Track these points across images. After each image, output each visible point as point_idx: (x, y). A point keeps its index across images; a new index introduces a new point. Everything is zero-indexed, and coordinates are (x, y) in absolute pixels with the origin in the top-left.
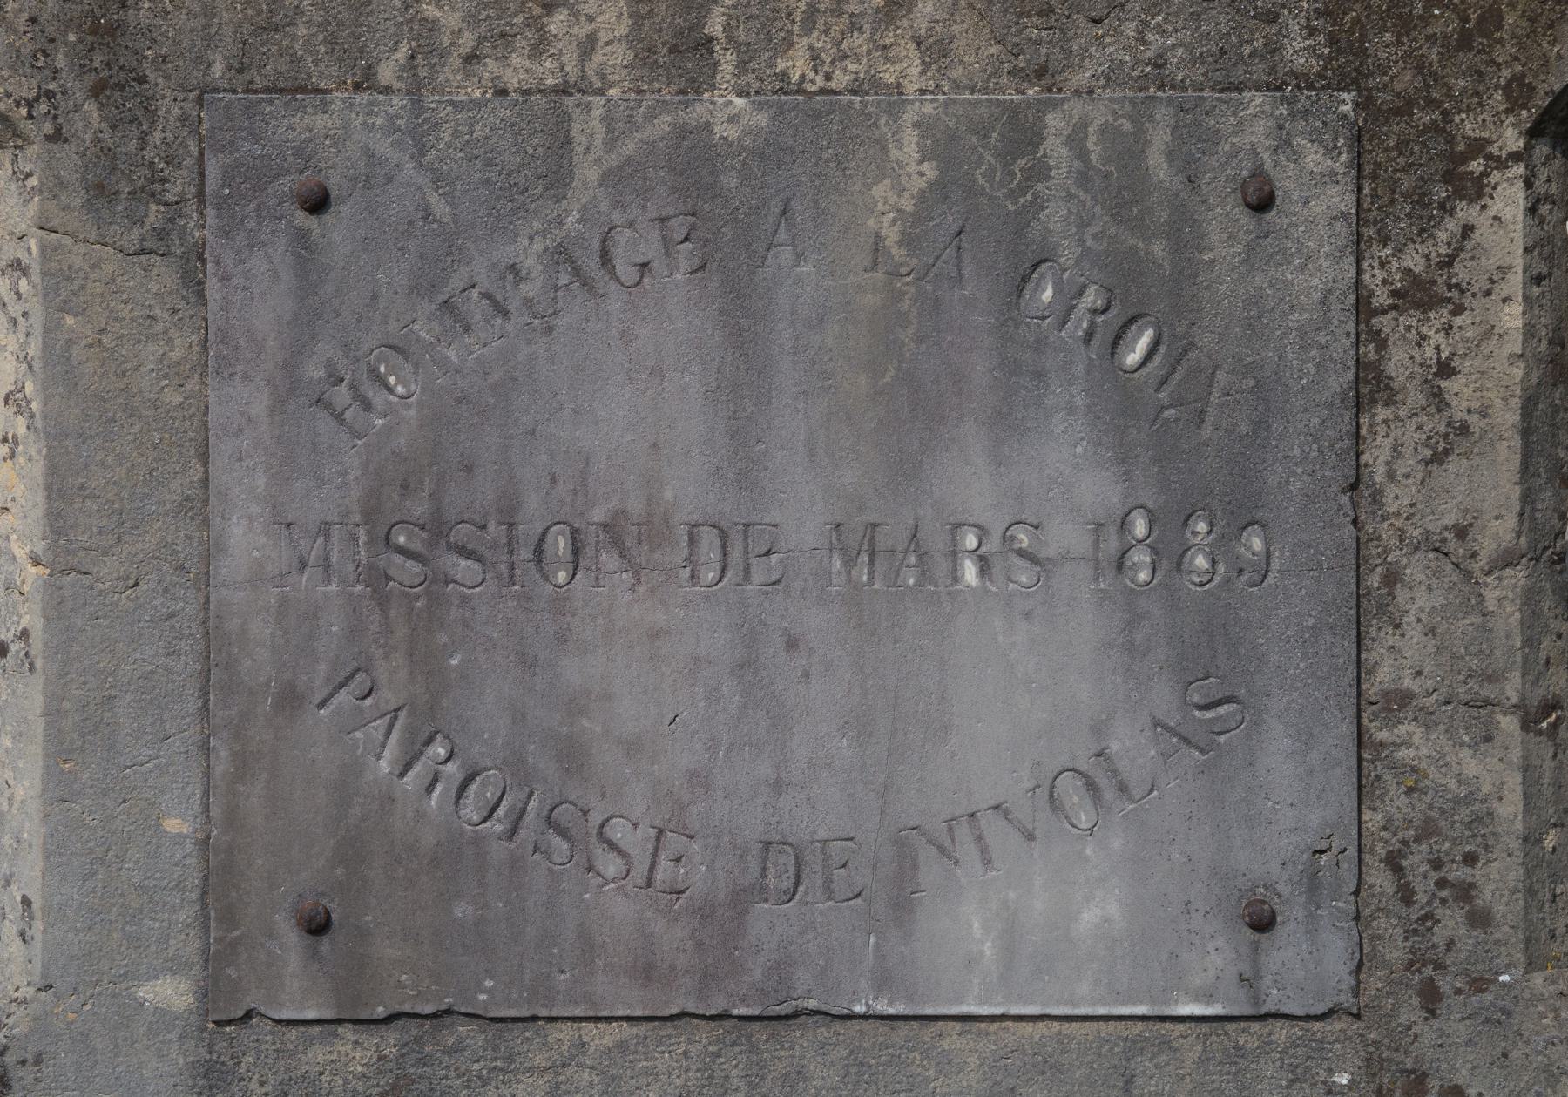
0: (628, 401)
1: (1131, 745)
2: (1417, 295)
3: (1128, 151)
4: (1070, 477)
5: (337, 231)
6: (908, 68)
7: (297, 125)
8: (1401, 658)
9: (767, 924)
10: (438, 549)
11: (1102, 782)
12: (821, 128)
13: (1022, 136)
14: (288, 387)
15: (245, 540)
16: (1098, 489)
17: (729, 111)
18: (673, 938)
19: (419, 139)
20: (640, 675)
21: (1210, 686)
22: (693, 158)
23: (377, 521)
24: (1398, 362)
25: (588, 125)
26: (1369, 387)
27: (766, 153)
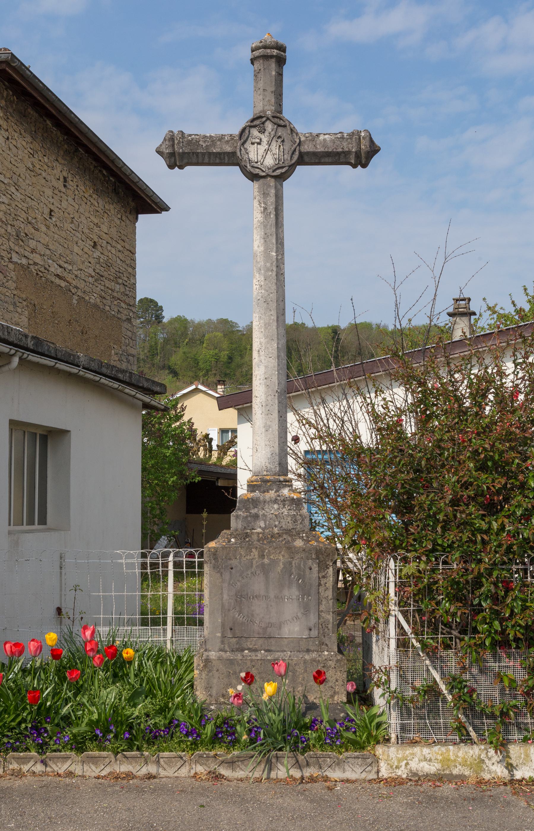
0: (258, 585)
1: (300, 615)
2: (324, 577)
3: (300, 565)
4: (295, 592)
5: (233, 571)
6: (281, 557)
8: (322, 608)
9: (269, 630)
10: (241, 597)
11: (297, 618)
12: (274, 562)
13: (291, 563)
14: (229, 584)
15: (225, 597)
16: (297, 593)
17: (266, 561)
18: (261, 631)
19: (240, 563)
20: (258, 608)
21: (306, 609)
22: (263, 565)
23: (236, 595)
24: (322, 583)
25: (254, 562)
27: (269, 565)
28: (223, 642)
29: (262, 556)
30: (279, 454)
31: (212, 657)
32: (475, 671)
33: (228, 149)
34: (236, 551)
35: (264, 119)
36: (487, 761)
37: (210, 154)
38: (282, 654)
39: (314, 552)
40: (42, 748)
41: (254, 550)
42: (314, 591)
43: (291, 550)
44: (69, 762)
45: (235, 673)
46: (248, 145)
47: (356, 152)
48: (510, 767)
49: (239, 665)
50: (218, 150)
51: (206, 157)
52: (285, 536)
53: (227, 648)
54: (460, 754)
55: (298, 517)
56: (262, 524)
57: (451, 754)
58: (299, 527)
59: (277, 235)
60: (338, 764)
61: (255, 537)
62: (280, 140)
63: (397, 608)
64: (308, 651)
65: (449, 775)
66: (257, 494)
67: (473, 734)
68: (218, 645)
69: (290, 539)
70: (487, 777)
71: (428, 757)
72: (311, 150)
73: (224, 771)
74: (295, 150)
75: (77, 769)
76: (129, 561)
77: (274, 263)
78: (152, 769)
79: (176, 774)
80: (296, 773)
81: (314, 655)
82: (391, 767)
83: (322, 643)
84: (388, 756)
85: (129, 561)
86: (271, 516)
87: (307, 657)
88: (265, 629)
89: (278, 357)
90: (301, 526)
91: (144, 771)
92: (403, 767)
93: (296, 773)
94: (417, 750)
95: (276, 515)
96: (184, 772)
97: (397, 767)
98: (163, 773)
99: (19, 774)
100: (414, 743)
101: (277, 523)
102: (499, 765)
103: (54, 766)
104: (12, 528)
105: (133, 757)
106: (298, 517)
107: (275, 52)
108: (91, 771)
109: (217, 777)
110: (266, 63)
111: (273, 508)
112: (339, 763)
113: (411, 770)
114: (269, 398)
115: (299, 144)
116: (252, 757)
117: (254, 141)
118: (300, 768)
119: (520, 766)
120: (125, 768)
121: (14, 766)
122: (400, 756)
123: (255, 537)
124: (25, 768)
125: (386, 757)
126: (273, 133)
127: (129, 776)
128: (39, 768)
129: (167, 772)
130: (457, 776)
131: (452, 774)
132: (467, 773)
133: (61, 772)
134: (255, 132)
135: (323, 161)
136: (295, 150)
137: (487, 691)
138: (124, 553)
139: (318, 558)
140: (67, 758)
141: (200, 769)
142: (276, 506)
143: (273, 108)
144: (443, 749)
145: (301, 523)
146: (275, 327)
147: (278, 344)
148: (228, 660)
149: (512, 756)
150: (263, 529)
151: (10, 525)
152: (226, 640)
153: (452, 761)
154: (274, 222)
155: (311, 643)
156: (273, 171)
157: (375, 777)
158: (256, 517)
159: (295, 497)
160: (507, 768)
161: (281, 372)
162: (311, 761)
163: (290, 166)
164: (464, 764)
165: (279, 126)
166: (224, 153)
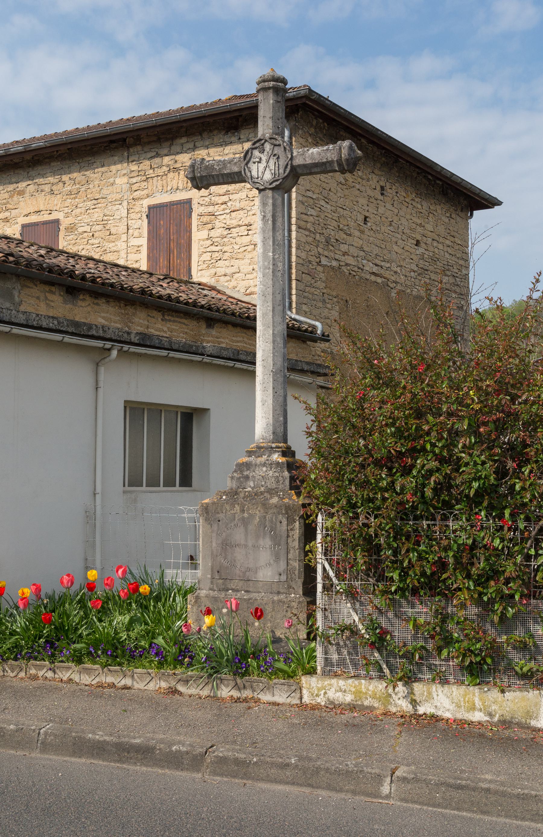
0: (239, 535)
1: (272, 561)
2: (292, 530)
3: (272, 519)
4: (267, 542)
5: (220, 523)
6: (258, 512)
7: (218, 515)
8: (290, 556)
9: (247, 573)
10: (227, 546)
11: (270, 564)
12: (252, 516)
13: (265, 517)
14: (217, 534)
15: (214, 545)
16: (270, 543)
17: (246, 515)
18: (241, 574)
19: (226, 516)
20: (239, 555)
21: (277, 558)
22: (243, 519)
23: (222, 544)
24: (290, 534)
25: (236, 516)
26: (288, 536)
27: (248, 518)
28: (212, 583)
29: (243, 511)
30: (273, 424)
31: (201, 595)
32: (391, 615)
33: (236, 169)
34: (222, 506)
35: (263, 141)
36: (394, 696)
37: (223, 175)
38: (257, 594)
39: (284, 508)
40: (52, 658)
41: (236, 506)
42: (283, 542)
43: (265, 506)
44: (70, 672)
45: (218, 609)
46: (251, 165)
47: (337, 161)
48: (414, 703)
49: (221, 602)
50: (228, 171)
51: (220, 178)
52: (266, 494)
53: (215, 588)
54: (371, 688)
55: (281, 478)
56: (252, 485)
57: (363, 687)
58: (281, 486)
59: (274, 238)
60: (268, 689)
61: (242, 495)
62: (275, 158)
63: (323, 557)
64: (279, 593)
65: (360, 705)
66: (252, 459)
67: (387, 671)
68: (209, 585)
69: (269, 496)
70: (394, 710)
71: (343, 688)
72: (302, 163)
73: (181, 688)
74: (287, 164)
75: (76, 677)
76: (190, 515)
77: (271, 262)
78: (128, 681)
79: (146, 688)
80: (235, 694)
81: (282, 597)
82: (312, 695)
83: (290, 587)
84: (310, 685)
85: (190, 515)
86: (259, 477)
87: (276, 598)
88: (244, 573)
89: (274, 342)
90: (283, 486)
91: (123, 682)
92: (322, 695)
93: (235, 694)
94: (334, 681)
95: (263, 477)
96: (152, 686)
97: (317, 695)
98: (136, 686)
99: (35, 678)
100: (336, 675)
101: (263, 483)
102: (405, 700)
103: (60, 674)
104: (127, 488)
105: (115, 671)
106: (281, 478)
107: (272, 84)
108: (86, 679)
109: (174, 691)
110: (266, 94)
111: (262, 470)
112: (268, 688)
113: (328, 699)
114: (266, 377)
115: (292, 159)
116: (202, 678)
117: (254, 160)
118: (239, 689)
119: (423, 702)
120: (110, 679)
121: (33, 671)
122: (320, 686)
123: (242, 495)
124: (41, 673)
125: (308, 686)
126: (270, 152)
127: (112, 686)
128: (50, 674)
129: (139, 685)
130: (367, 707)
131: (363, 705)
132: (376, 705)
133: (65, 679)
134: (256, 153)
135: (313, 171)
136: (287, 164)
137: (401, 633)
138: (185, 509)
139: (287, 513)
140: (69, 668)
141: (164, 685)
142: (264, 469)
143: (271, 131)
144: (357, 682)
145: (283, 483)
146: (271, 316)
147: (273, 330)
148: (213, 597)
149: (416, 693)
150: (253, 488)
151: (124, 486)
152: (214, 580)
153: (364, 693)
154: (271, 227)
155: (281, 586)
156: (270, 184)
157: (298, 702)
158: (247, 478)
159: (280, 461)
160: (411, 703)
161: (276, 354)
162: (247, 684)
163: (283, 179)
164: (374, 697)
165: (275, 145)
166: (234, 173)
